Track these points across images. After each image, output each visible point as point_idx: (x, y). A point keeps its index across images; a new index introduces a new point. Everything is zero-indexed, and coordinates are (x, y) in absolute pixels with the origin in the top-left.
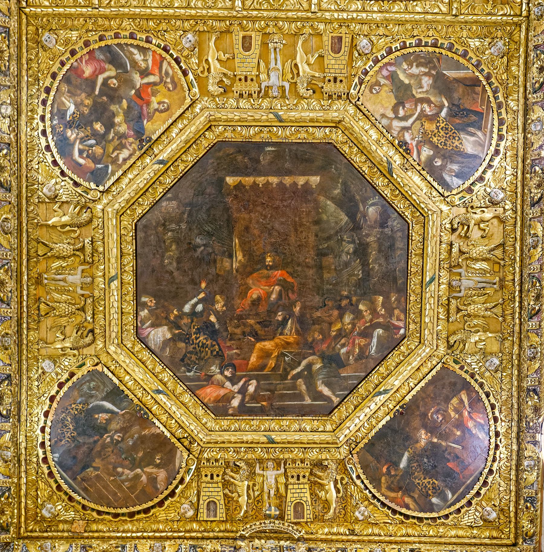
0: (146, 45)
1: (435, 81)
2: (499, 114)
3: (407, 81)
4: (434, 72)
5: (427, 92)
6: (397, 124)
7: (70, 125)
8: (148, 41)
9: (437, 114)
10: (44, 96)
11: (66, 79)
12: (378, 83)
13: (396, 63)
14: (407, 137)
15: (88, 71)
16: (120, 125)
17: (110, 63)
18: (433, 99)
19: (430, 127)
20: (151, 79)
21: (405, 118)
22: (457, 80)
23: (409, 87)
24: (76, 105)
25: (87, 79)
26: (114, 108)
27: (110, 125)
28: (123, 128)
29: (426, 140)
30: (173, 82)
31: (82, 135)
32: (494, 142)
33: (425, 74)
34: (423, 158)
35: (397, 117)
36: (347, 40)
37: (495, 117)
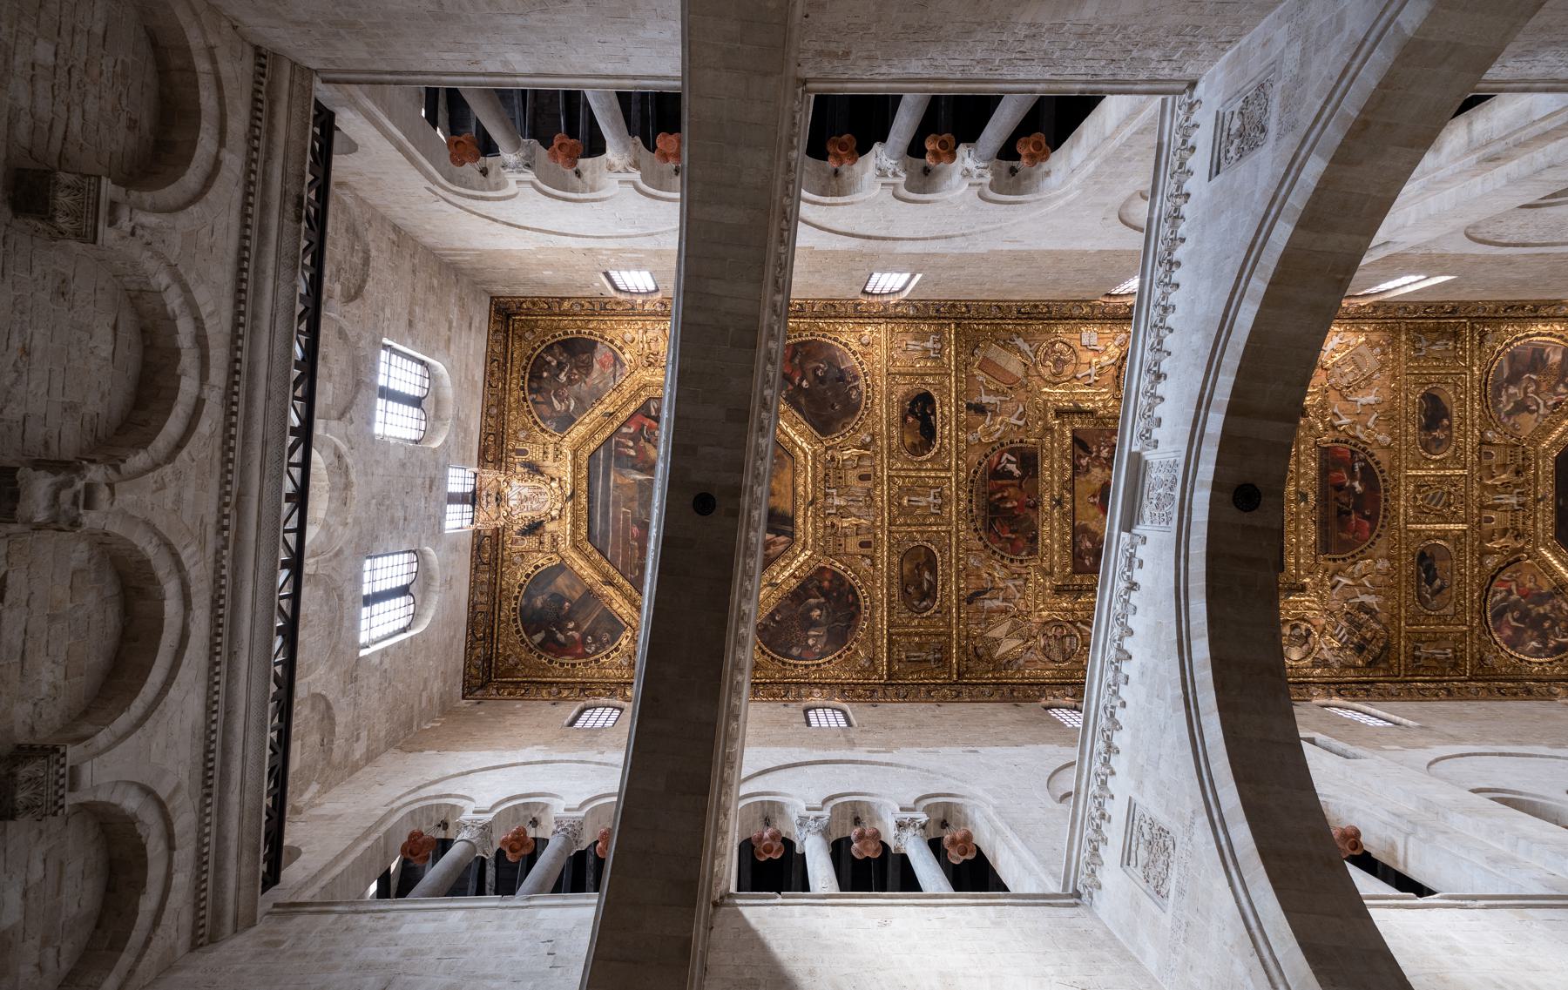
0: (1491, 593)
1: (1512, 384)
2: (1533, 336)
3: (1512, 404)
4: (1505, 385)
5: (1519, 389)
6: (1541, 412)
7: (1545, 645)
8: (1488, 590)
9: (1535, 381)
10: (1524, 663)
11: (1513, 648)
12: (1514, 424)
13: (1499, 412)
14: (1550, 403)
15: (1508, 632)
16: (1545, 610)
17: (1502, 616)
18: (1524, 385)
19: (1544, 387)
20: (1514, 587)
21: (1538, 405)
22: (1511, 368)
23: (1516, 403)
24: (1533, 640)
25: (1514, 633)
26: (1534, 613)
27: (1545, 617)
28: (1548, 607)
29: (1553, 389)
30: (1515, 572)
31: (1552, 637)
32: (1553, 340)
33: (1507, 391)
34: (1565, 391)
35: (1537, 411)
36: (1485, 449)
37: (1535, 339)
